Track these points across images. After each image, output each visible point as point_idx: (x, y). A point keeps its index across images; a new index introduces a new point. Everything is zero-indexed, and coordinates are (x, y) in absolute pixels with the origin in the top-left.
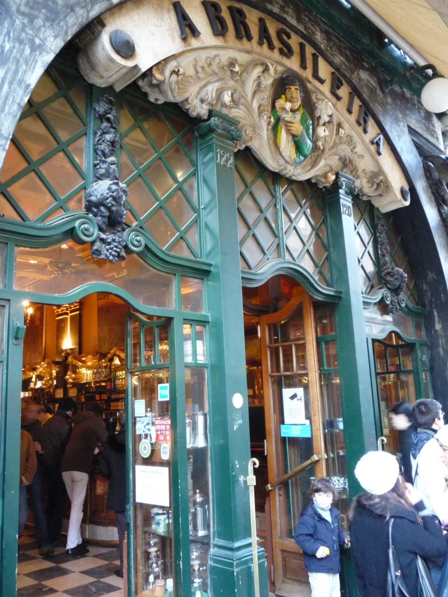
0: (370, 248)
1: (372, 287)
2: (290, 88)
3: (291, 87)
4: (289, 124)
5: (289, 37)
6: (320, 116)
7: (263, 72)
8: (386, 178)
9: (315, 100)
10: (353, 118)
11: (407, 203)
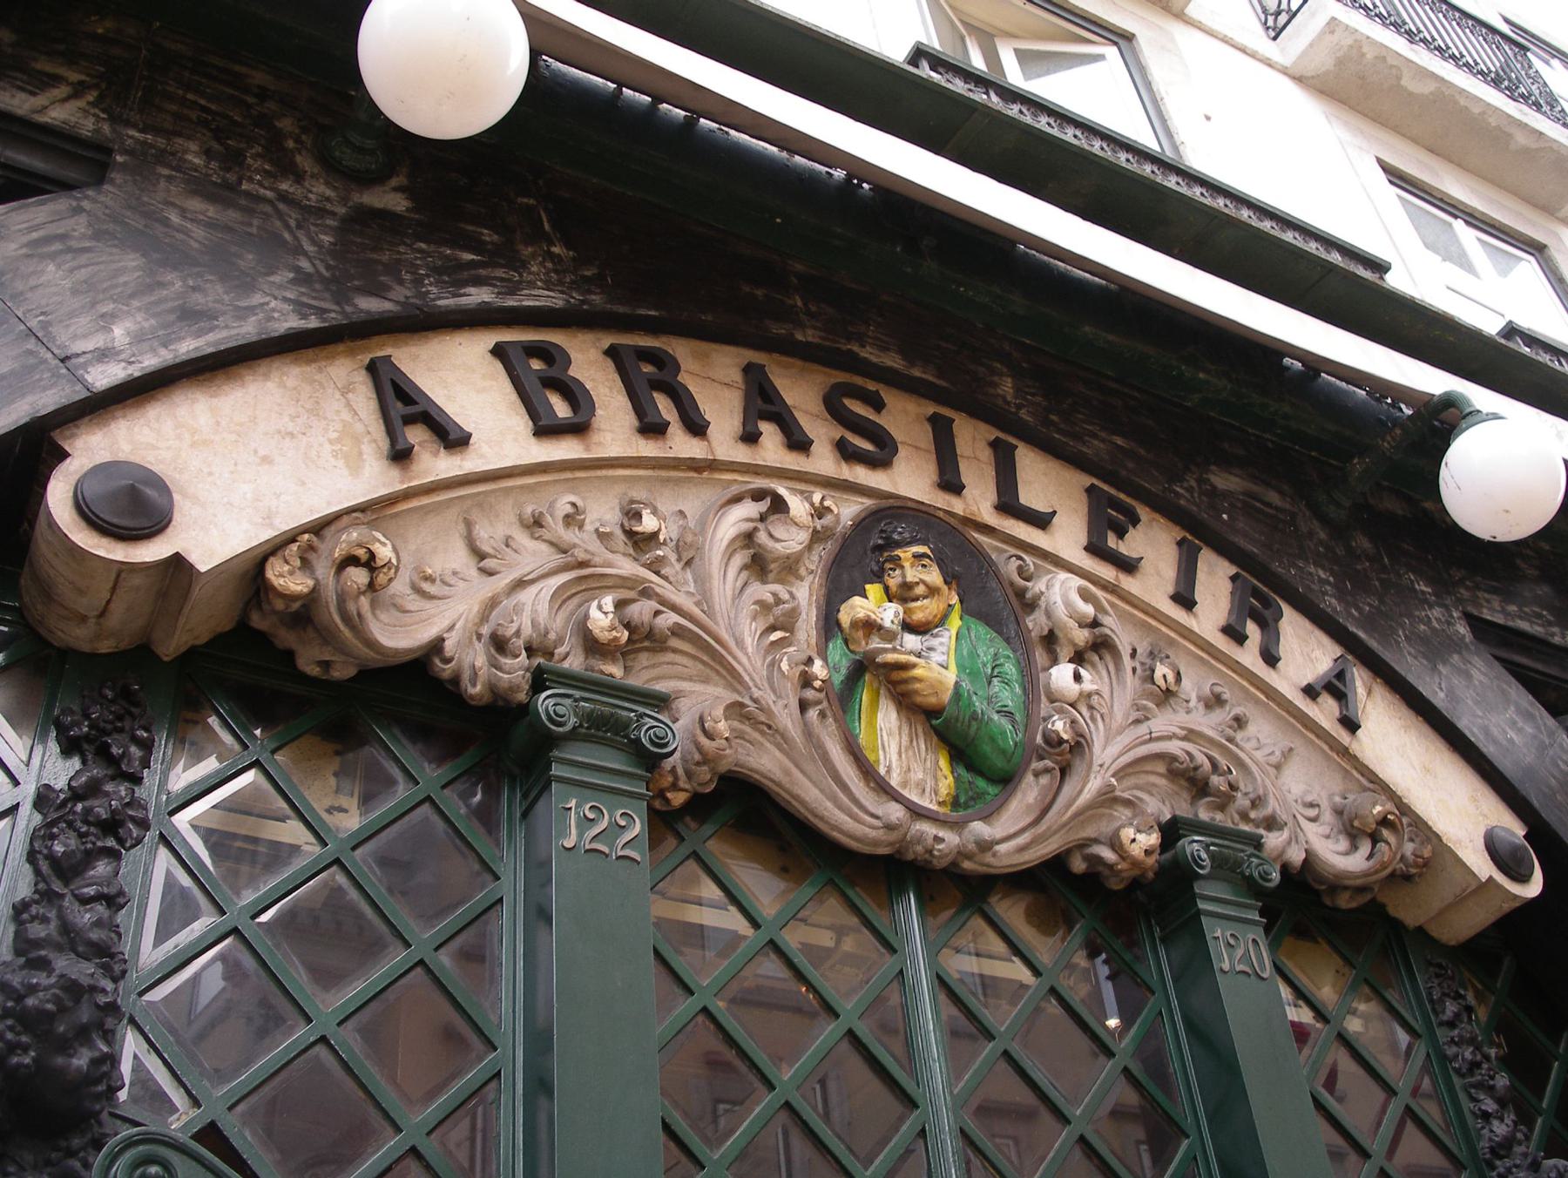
4: (897, 675)
5: (878, 406)
6: (1051, 632)
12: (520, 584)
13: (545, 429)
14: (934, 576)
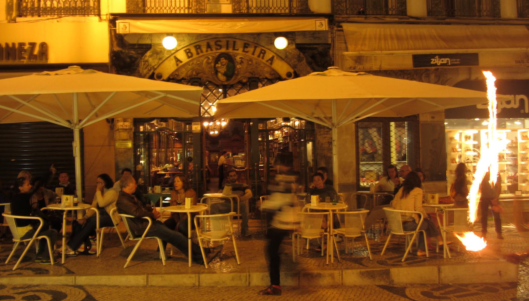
12: (189, 71)
13: (189, 57)
14: (224, 61)
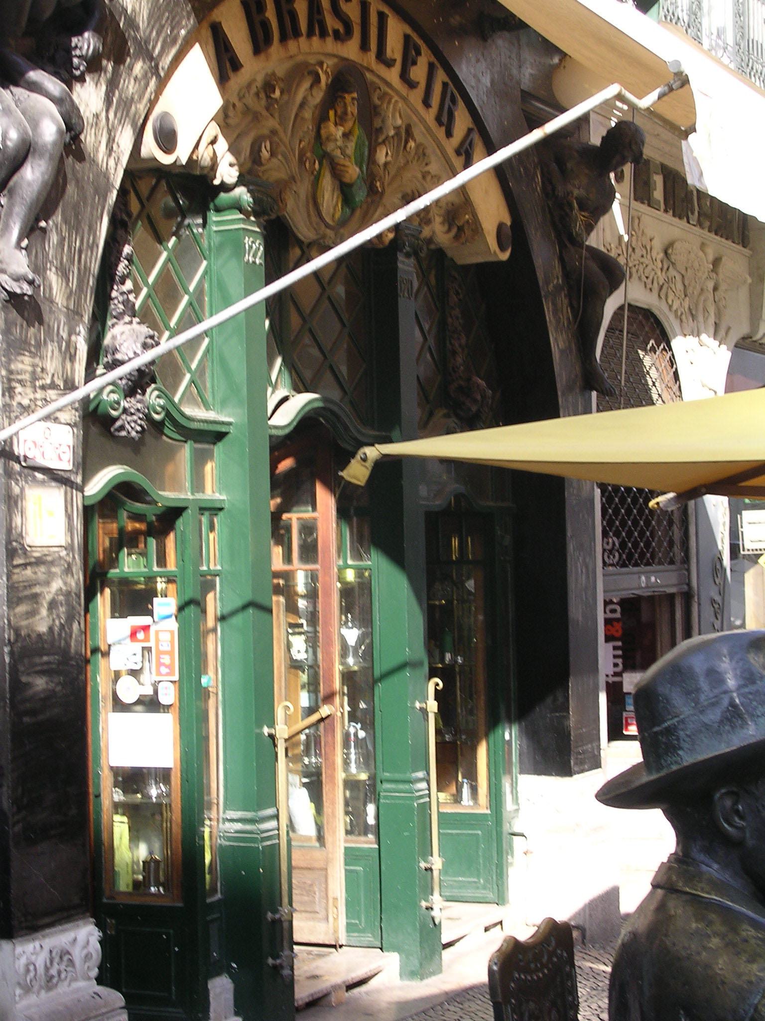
0: (431, 342)
1: (431, 414)
2: (345, 98)
3: (346, 96)
6: (381, 128)
7: (312, 87)
8: (474, 215)
9: (377, 102)
10: (430, 116)
11: (505, 256)
